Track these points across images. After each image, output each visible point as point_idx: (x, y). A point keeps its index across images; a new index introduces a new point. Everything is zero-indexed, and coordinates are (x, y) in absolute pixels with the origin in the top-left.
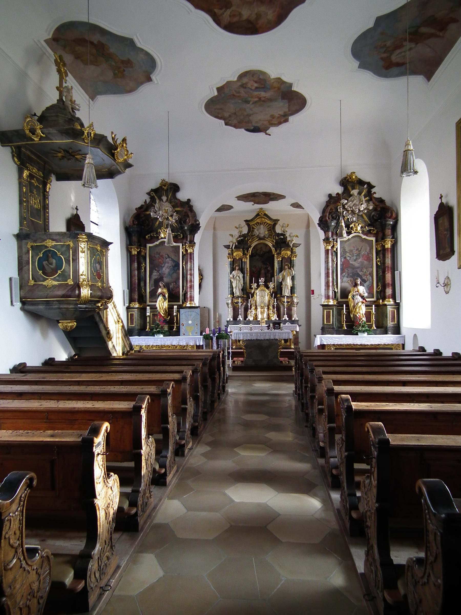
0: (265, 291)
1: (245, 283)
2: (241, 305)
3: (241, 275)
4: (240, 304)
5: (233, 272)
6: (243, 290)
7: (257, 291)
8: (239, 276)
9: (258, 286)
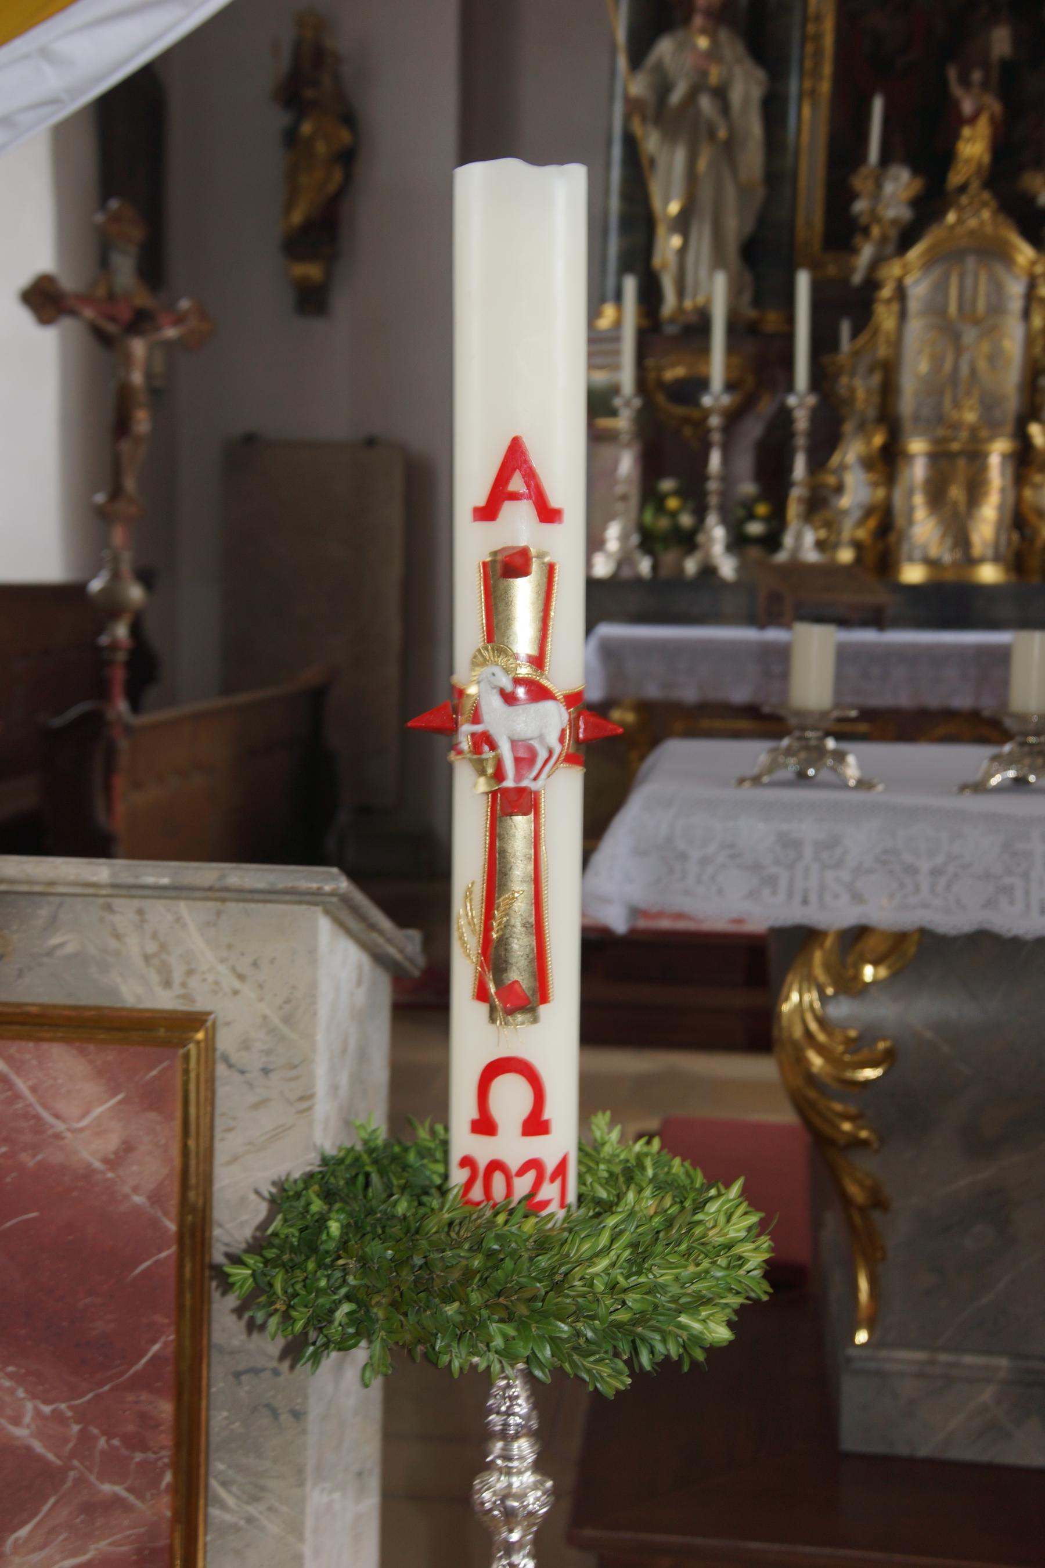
0: (1003, 255)
1: (778, 176)
2: (733, 418)
3: (746, 87)
4: (716, 397)
5: (665, 48)
6: (763, 260)
7: (913, 275)
8: (721, 94)
9: (929, 206)
